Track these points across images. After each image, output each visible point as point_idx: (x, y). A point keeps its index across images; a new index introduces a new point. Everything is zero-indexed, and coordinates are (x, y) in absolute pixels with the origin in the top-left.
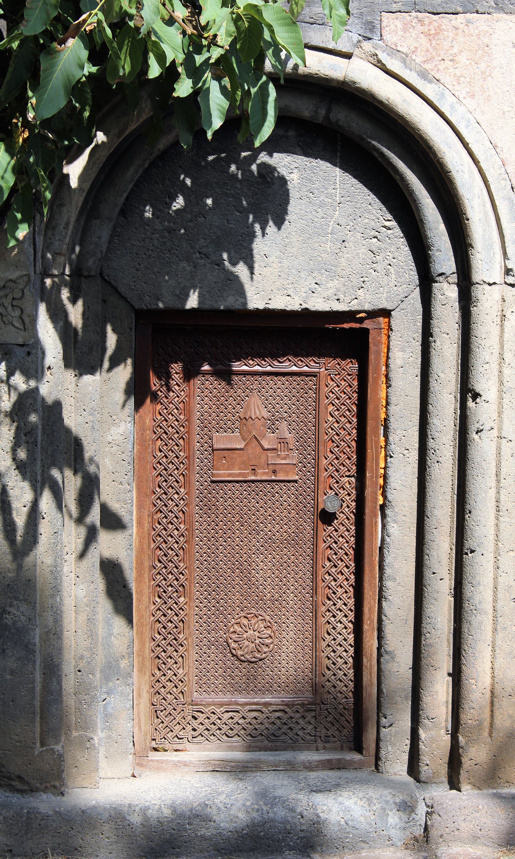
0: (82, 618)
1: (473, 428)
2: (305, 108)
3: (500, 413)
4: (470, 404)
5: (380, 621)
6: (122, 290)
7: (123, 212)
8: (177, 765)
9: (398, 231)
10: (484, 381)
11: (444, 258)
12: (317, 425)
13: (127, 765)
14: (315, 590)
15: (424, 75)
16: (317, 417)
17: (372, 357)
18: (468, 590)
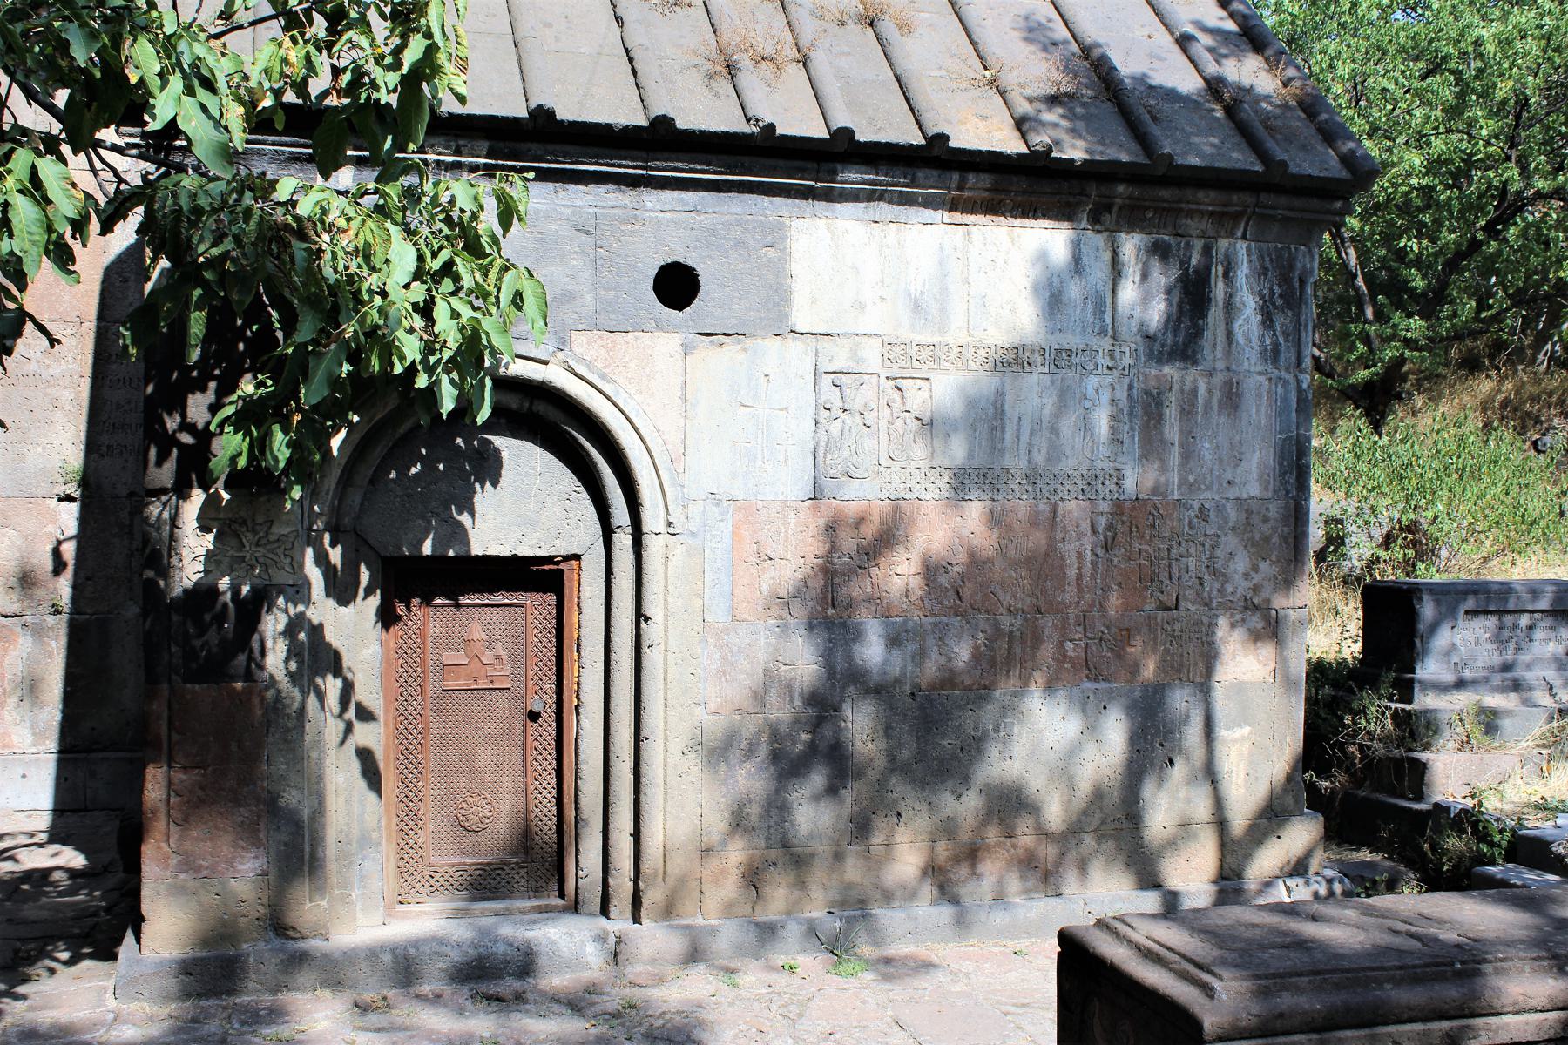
0: (341, 800)
1: (645, 644)
2: (513, 401)
3: (666, 632)
4: (643, 625)
5: (576, 796)
6: (372, 542)
7: (372, 482)
8: (418, 914)
9: (585, 495)
10: (652, 607)
11: (620, 514)
12: (525, 645)
13: (378, 915)
14: (525, 773)
15: (603, 377)
16: (525, 639)
17: (567, 591)
18: (644, 769)
